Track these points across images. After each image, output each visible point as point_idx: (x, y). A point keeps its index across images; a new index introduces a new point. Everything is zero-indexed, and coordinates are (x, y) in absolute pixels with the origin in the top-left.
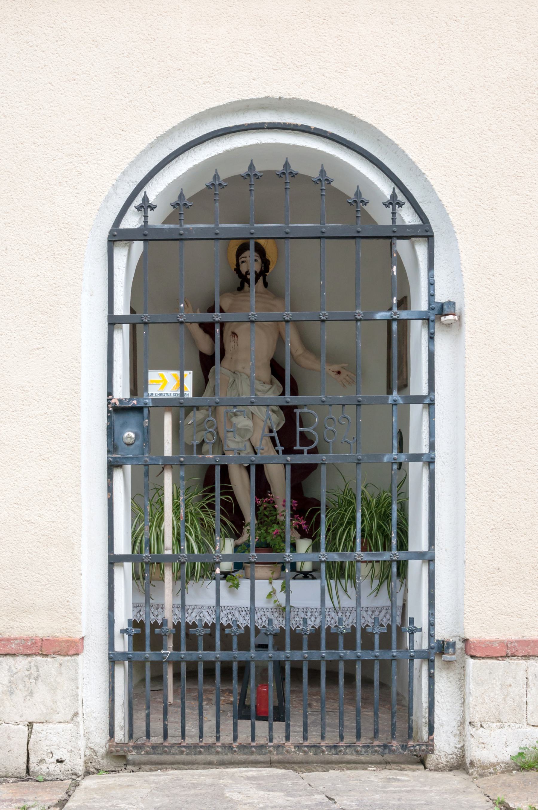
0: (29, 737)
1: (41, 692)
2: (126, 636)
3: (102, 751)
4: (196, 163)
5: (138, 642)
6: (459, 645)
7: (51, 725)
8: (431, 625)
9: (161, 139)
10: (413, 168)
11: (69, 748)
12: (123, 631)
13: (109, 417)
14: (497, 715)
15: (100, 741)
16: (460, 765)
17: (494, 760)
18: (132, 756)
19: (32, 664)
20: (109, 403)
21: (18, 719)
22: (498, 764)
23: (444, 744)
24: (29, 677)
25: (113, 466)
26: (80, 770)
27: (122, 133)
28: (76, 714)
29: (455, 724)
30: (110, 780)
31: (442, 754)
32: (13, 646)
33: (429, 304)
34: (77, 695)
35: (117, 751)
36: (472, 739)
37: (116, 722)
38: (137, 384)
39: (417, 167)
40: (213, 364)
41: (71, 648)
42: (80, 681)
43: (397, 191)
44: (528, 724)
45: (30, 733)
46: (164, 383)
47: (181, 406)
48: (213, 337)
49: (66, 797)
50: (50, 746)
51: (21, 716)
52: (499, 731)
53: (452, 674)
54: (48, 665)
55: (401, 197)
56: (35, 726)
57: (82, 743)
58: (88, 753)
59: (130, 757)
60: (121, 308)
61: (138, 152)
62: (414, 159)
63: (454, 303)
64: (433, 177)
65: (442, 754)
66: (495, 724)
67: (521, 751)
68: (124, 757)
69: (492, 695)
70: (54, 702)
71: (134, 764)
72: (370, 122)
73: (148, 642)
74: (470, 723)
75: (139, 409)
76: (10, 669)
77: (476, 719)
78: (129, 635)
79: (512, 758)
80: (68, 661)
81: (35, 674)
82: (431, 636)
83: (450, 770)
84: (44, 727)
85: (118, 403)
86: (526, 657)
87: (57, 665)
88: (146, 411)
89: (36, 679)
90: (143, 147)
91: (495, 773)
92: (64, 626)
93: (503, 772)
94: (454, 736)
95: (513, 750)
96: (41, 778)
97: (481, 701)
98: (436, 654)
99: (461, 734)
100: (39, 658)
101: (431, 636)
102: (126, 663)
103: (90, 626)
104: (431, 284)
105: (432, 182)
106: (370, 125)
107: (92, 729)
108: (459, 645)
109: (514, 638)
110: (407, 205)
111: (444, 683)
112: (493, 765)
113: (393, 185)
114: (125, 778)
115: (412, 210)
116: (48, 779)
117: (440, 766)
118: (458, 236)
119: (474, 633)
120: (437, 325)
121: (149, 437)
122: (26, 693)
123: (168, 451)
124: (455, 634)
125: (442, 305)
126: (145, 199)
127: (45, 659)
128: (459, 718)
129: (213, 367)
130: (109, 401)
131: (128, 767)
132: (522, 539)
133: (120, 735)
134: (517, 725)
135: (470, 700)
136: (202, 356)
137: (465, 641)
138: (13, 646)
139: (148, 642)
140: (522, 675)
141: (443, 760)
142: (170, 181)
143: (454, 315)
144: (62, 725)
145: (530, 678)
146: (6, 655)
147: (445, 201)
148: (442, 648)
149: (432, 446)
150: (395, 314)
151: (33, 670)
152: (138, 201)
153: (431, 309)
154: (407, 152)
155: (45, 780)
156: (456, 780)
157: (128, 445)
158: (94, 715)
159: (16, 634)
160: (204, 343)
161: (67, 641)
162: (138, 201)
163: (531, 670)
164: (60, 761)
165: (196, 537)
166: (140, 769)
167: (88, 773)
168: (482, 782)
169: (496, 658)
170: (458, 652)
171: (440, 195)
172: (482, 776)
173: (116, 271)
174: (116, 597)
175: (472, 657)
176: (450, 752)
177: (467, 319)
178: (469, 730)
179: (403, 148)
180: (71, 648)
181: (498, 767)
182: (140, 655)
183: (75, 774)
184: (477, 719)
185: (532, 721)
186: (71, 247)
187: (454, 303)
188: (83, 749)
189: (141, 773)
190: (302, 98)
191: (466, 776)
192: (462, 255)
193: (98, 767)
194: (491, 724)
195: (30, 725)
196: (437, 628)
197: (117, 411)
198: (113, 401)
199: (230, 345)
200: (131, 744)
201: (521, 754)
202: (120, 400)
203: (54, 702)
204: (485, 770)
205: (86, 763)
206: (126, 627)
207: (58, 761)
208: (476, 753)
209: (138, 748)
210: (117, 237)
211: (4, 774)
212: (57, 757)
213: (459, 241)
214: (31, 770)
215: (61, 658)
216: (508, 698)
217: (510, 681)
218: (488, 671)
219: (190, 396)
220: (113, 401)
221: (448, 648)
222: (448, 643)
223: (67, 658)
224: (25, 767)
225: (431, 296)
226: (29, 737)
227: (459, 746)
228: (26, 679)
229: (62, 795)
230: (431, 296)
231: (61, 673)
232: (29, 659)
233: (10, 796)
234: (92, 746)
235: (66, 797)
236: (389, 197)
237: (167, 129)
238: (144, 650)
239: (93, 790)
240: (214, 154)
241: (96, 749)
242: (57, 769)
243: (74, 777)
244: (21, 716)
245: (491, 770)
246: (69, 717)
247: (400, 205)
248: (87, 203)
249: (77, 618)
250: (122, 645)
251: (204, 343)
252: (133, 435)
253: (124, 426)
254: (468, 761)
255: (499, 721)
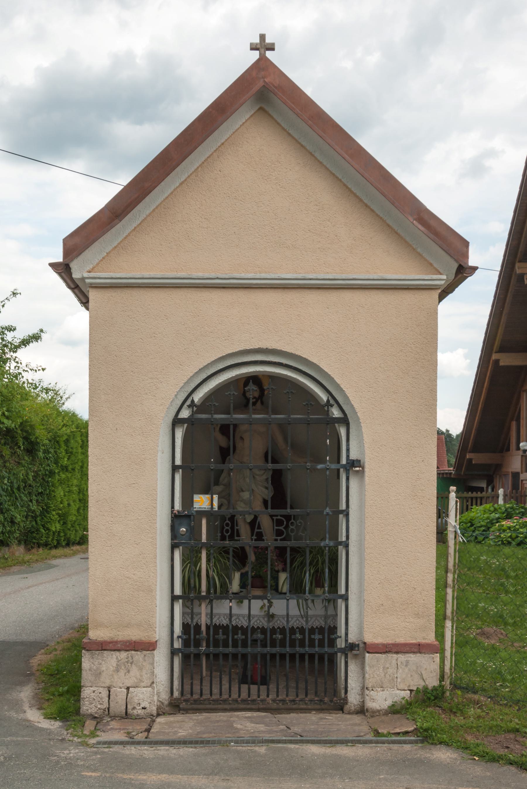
0: (127, 695)
1: (134, 671)
2: (180, 639)
3: (166, 703)
4: (220, 381)
5: (186, 643)
6: (361, 645)
7: (139, 689)
8: (347, 634)
9: (201, 370)
10: (338, 387)
11: (149, 701)
12: (179, 637)
13: (172, 521)
14: (381, 684)
15: (165, 696)
16: (362, 711)
17: (379, 708)
18: (183, 705)
19: (129, 655)
20: (172, 513)
21: (121, 685)
22: (381, 710)
23: (353, 698)
24: (127, 662)
25: (173, 547)
26: (155, 713)
27: (180, 366)
28: (153, 683)
29: (359, 688)
30: (171, 718)
31: (352, 705)
32: (119, 645)
33: (347, 461)
34: (154, 672)
35: (175, 703)
36: (367, 697)
37: (174, 687)
38: (187, 501)
39: (340, 387)
40: (229, 455)
41: (150, 646)
42: (155, 664)
43: (330, 398)
44: (397, 689)
45: (128, 693)
46: (202, 502)
47: (212, 514)
48: (229, 439)
49: (149, 727)
50: (139, 700)
51: (123, 684)
52: (381, 692)
53: (358, 661)
54: (138, 656)
55: (332, 402)
56: (131, 689)
57: (156, 698)
58: (158, 704)
59: (181, 706)
60: (178, 462)
61: (189, 377)
62: (339, 383)
63: (360, 461)
64: (349, 393)
65: (352, 705)
66: (379, 689)
67: (393, 703)
68: (178, 706)
69: (378, 673)
70: (141, 676)
71: (184, 710)
72: (315, 362)
73: (192, 643)
74: (367, 688)
75: (188, 516)
76: (117, 658)
77: (370, 686)
78: (182, 639)
79: (389, 707)
80: (149, 654)
81: (131, 661)
82: (346, 641)
83: (356, 714)
84: (136, 689)
85: (177, 513)
86: (397, 653)
87: (143, 656)
88: (192, 517)
89: (131, 663)
90: (191, 374)
91: (380, 715)
92: (147, 634)
93: (384, 715)
94: (359, 695)
95: (389, 703)
96: (134, 717)
97: (372, 676)
98: (349, 650)
99: (362, 694)
100: (133, 652)
101: (346, 641)
102: (180, 654)
103: (161, 634)
104: (348, 450)
105: (348, 395)
106: (315, 364)
107: (161, 690)
108: (361, 645)
109: (390, 642)
110: (336, 405)
111: (353, 667)
112: (379, 711)
113: (328, 395)
114: (179, 717)
115: (338, 408)
116: (138, 718)
117: (351, 712)
118: (362, 425)
119: (369, 638)
120: (351, 472)
121: (194, 532)
122: (126, 671)
123: (204, 539)
124: (359, 639)
125: (353, 461)
126: (193, 401)
127: (136, 652)
128: (361, 685)
129: (229, 457)
130: (172, 512)
131: (181, 711)
132: (395, 588)
133: (176, 694)
134: (392, 690)
135: (367, 676)
136: (221, 448)
137: (365, 643)
138: (119, 645)
139: (192, 643)
140: (394, 662)
141: (353, 708)
142: (206, 391)
143: (359, 467)
144: (145, 689)
145: (399, 664)
146: (115, 650)
147: (356, 406)
148: (352, 647)
149: (348, 537)
150: (328, 466)
151: (130, 659)
152: (188, 402)
153: (347, 463)
154: (335, 379)
155: (136, 719)
156: (357, 719)
157: (183, 535)
158: (162, 683)
159: (120, 638)
160: (223, 441)
161: (149, 643)
162: (188, 402)
163: (399, 659)
164: (144, 708)
165: (218, 572)
166: (187, 713)
167: (158, 715)
168: (371, 720)
169: (381, 653)
170: (361, 649)
171: (352, 402)
172: (372, 717)
173: (176, 440)
174: (175, 618)
175: (368, 652)
176: (356, 704)
177: (367, 470)
178: (367, 692)
179: (333, 376)
180: (150, 646)
181: (381, 712)
182: (187, 650)
183: (152, 715)
184: (370, 686)
185: (399, 687)
186: (152, 428)
187: (360, 461)
188: (156, 702)
189: (188, 715)
190: (278, 349)
191: (364, 717)
192: (364, 435)
193: (164, 711)
194: (377, 689)
195: (128, 688)
196: (350, 636)
197: (176, 519)
198: (174, 512)
199: (239, 445)
200: (182, 699)
201: (393, 705)
202: (178, 511)
203: (141, 676)
204: (375, 713)
205: (157, 709)
206: (180, 635)
207: (143, 708)
208: (370, 705)
209: (186, 701)
210: (176, 422)
211: (113, 715)
212: (142, 706)
213: (363, 427)
214: (128, 713)
215: (145, 652)
216: (387, 675)
217: (388, 665)
218: (376, 660)
219: (216, 509)
220: (174, 512)
221: (355, 647)
222: (355, 645)
223: (148, 652)
224: (124, 711)
225: (348, 456)
226: (127, 695)
227: (361, 700)
228: (126, 664)
229: (146, 726)
230: (348, 456)
231: (145, 660)
232: (128, 653)
233: (118, 727)
234: (161, 700)
235: (149, 727)
236: (325, 401)
237: (205, 364)
238: (190, 647)
239: (163, 723)
240: (230, 376)
241: (163, 701)
242: (142, 713)
243: (151, 717)
244: (123, 684)
245: (377, 714)
246: (149, 684)
247: (332, 406)
248: (161, 405)
249: (154, 630)
250: (177, 645)
251: (223, 441)
252: (184, 530)
253: (181, 525)
254: (365, 709)
255: (382, 687)
